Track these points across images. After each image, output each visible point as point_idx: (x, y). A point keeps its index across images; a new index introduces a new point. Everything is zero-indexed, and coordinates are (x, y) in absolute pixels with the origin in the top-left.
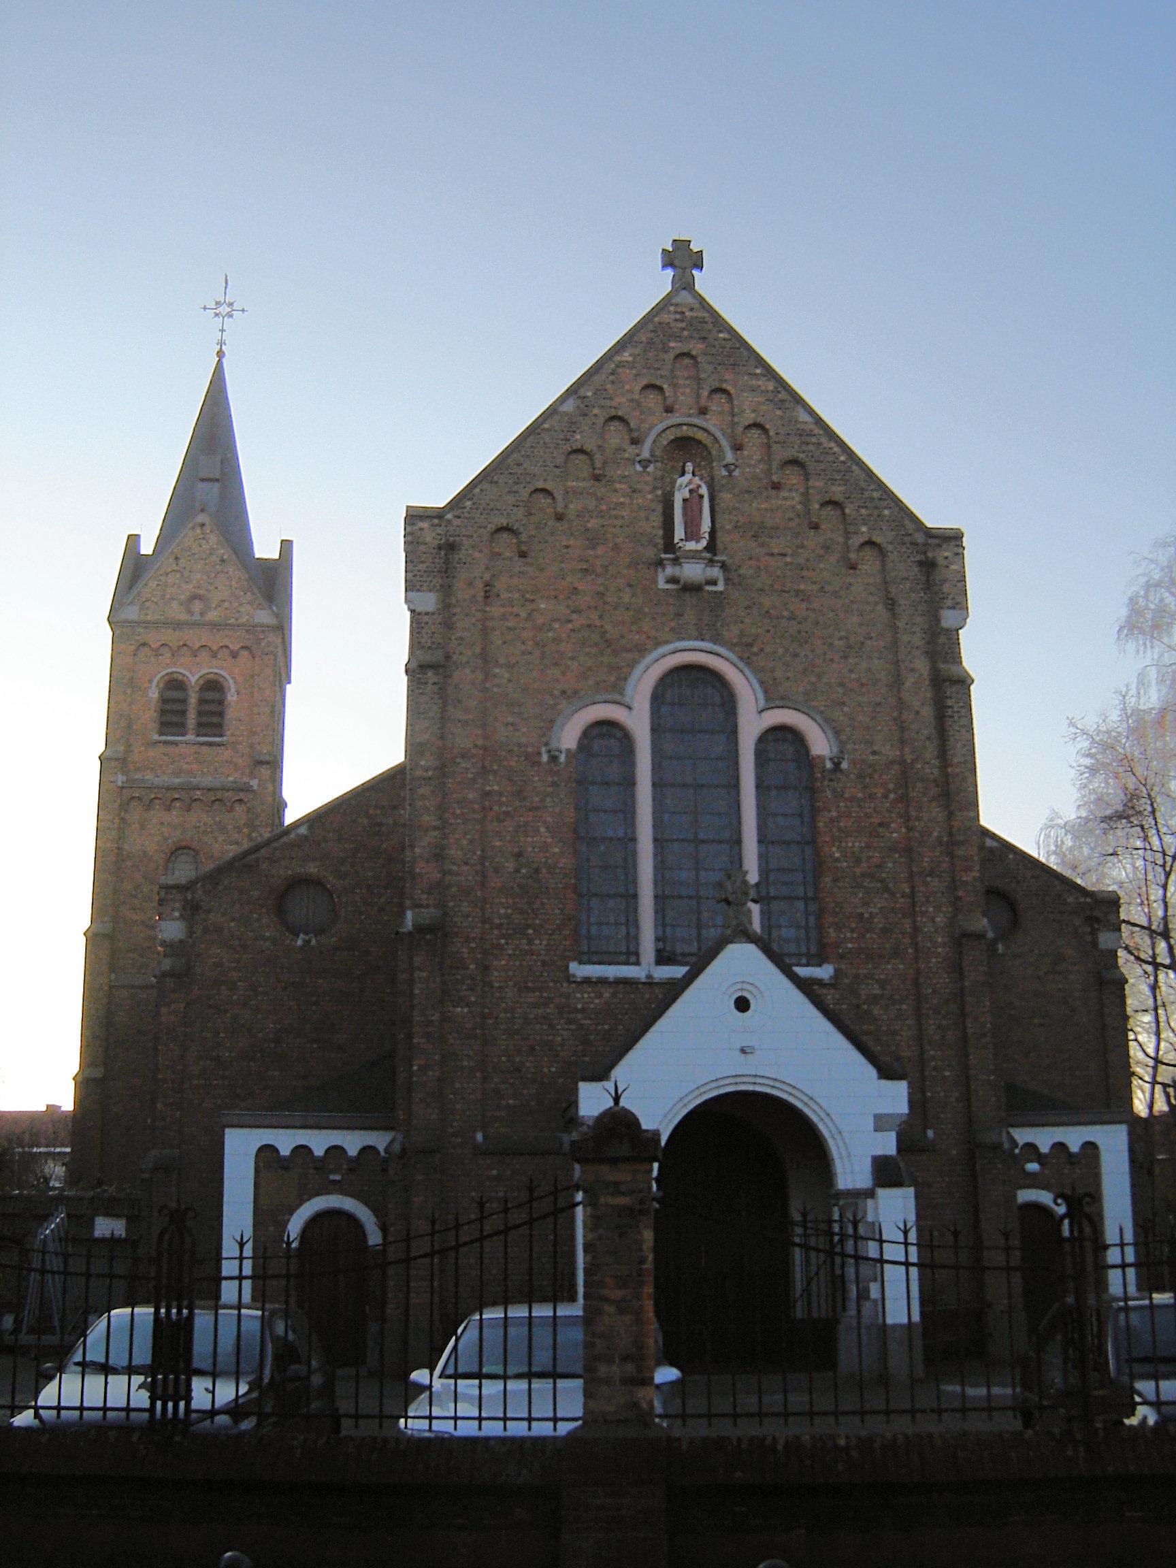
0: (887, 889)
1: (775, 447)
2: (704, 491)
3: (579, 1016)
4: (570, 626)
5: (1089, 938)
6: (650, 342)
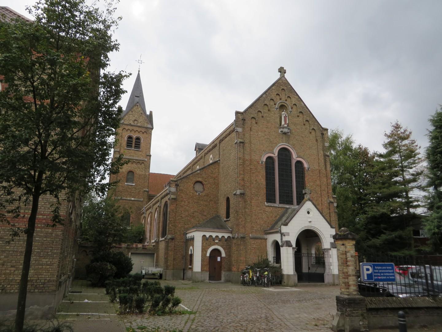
1: (298, 109)
2: (287, 115)
4: (264, 138)
6: (277, 86)
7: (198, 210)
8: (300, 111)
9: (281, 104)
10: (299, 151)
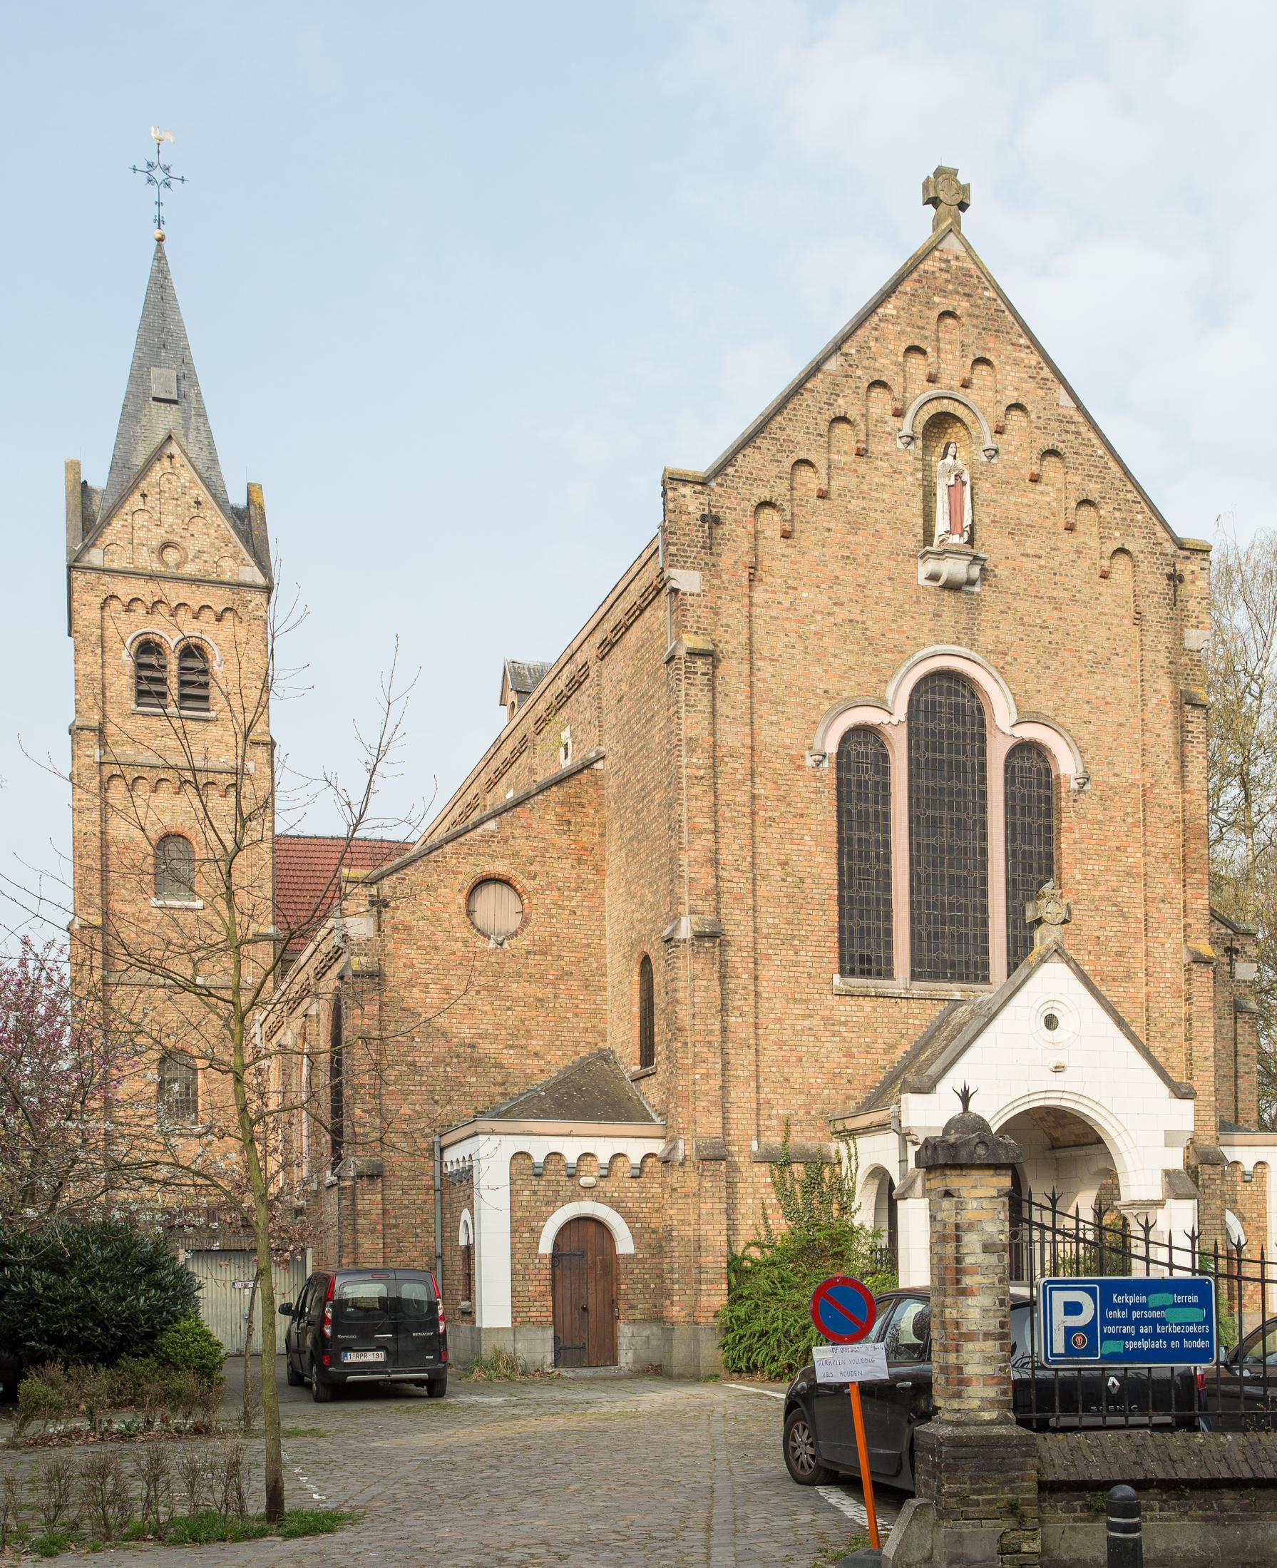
3: (843, 1029)
4: (832, 619)
7: (498, 1026)
8: (1048, 443)
9: (933, 409)
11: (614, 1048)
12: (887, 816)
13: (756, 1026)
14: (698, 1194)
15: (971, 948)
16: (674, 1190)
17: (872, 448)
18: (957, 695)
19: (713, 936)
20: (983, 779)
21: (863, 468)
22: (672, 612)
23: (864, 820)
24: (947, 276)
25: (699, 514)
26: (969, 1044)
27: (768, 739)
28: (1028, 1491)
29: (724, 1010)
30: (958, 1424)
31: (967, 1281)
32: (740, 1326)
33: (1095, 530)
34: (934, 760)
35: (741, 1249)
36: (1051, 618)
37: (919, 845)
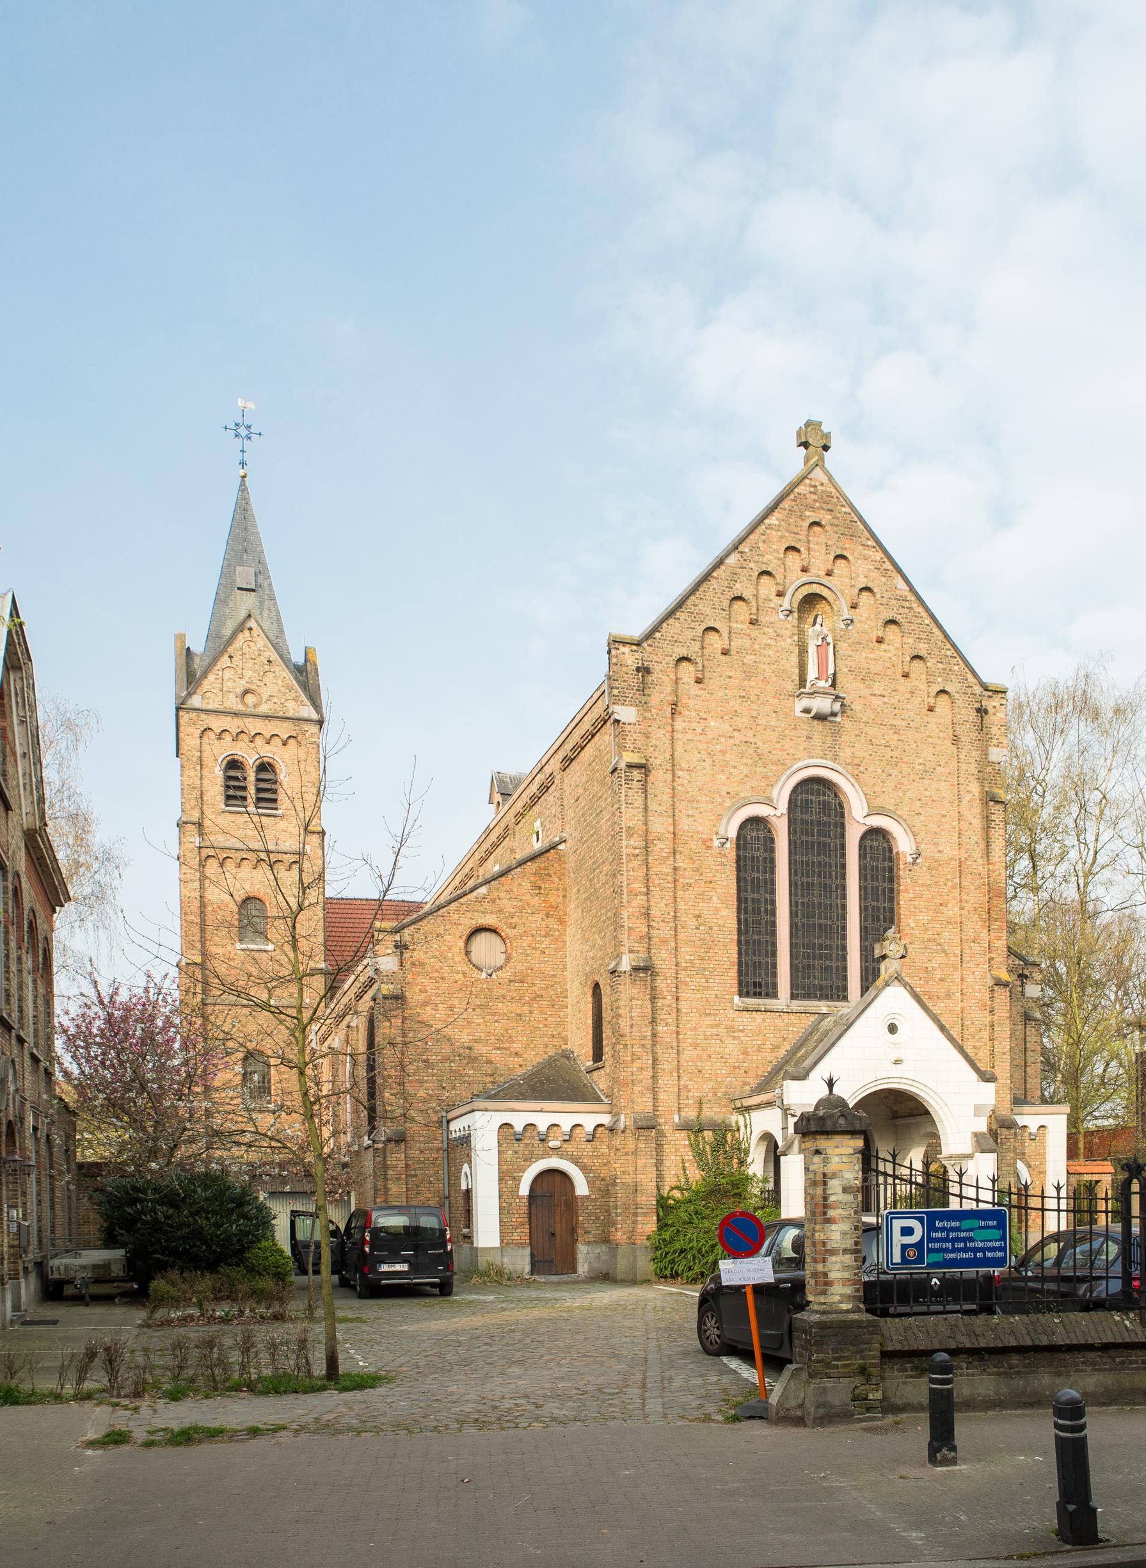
0: (945, 952)
3: (741, 1034)
4: (732, 741)
5: (1020, 989)
7: (488, 1034)
8: (890, 615)
9: (806, 590)
10: (876, 789)
11: (573, 1049)
12: (773, 882)
13: (678, 1033)
14: (635, 1153)
15: (835, 976)
16: (618, 1150)
17: (761, 618)
18: (824, 795)
19: (645, 969)
20: (843, 855)
21: (754, 632)
22: (615, 737)
23: (756, 885)
24: (815, 497)
25: (635, 666)
26: (833, 1044)
27: (686, 827)
28: (874, 1358)
29: (653, 1021)
30: (824, 1313)
31: (831, 1213)
32: (666, 1246)
33: (924, 677)
34: (807, 842)
35: (666, 1191)
36: (893, 740)
37: (796, 903)
